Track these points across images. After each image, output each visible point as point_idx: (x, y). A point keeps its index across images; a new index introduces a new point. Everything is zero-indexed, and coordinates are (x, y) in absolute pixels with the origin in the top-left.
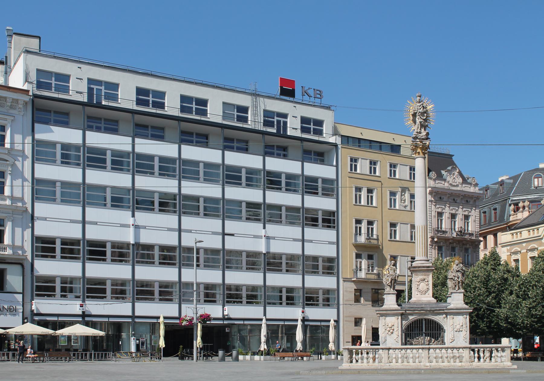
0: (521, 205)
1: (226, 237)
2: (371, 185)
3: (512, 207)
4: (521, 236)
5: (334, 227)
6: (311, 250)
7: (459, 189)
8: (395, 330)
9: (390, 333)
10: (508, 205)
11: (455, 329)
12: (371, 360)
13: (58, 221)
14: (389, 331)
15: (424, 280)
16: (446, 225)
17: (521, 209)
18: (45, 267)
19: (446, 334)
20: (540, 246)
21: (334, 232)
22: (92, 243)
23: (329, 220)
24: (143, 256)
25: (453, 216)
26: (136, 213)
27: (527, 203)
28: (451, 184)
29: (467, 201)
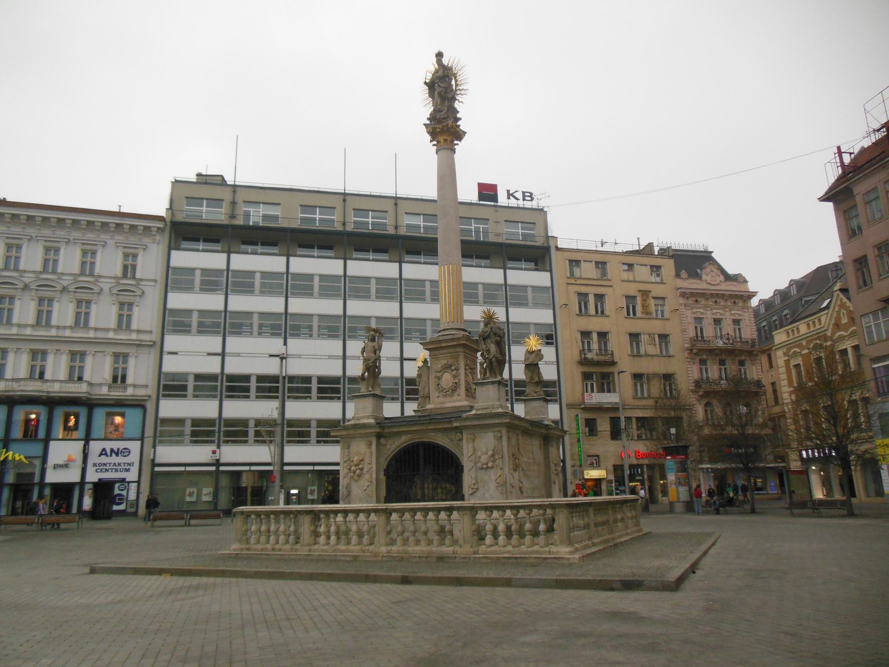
1: (405, 362)
2: (599, 290)
4: (798, 332)
8: (366, 470)
9: (355, 477)
11: (479, 465)
12: (282, 538)
13: (191, 354)
16: (709, 332)
18: (171, 408)
22: (232, 378)
24: (298, 390)
25: (717, 321)
26: (289, 341)
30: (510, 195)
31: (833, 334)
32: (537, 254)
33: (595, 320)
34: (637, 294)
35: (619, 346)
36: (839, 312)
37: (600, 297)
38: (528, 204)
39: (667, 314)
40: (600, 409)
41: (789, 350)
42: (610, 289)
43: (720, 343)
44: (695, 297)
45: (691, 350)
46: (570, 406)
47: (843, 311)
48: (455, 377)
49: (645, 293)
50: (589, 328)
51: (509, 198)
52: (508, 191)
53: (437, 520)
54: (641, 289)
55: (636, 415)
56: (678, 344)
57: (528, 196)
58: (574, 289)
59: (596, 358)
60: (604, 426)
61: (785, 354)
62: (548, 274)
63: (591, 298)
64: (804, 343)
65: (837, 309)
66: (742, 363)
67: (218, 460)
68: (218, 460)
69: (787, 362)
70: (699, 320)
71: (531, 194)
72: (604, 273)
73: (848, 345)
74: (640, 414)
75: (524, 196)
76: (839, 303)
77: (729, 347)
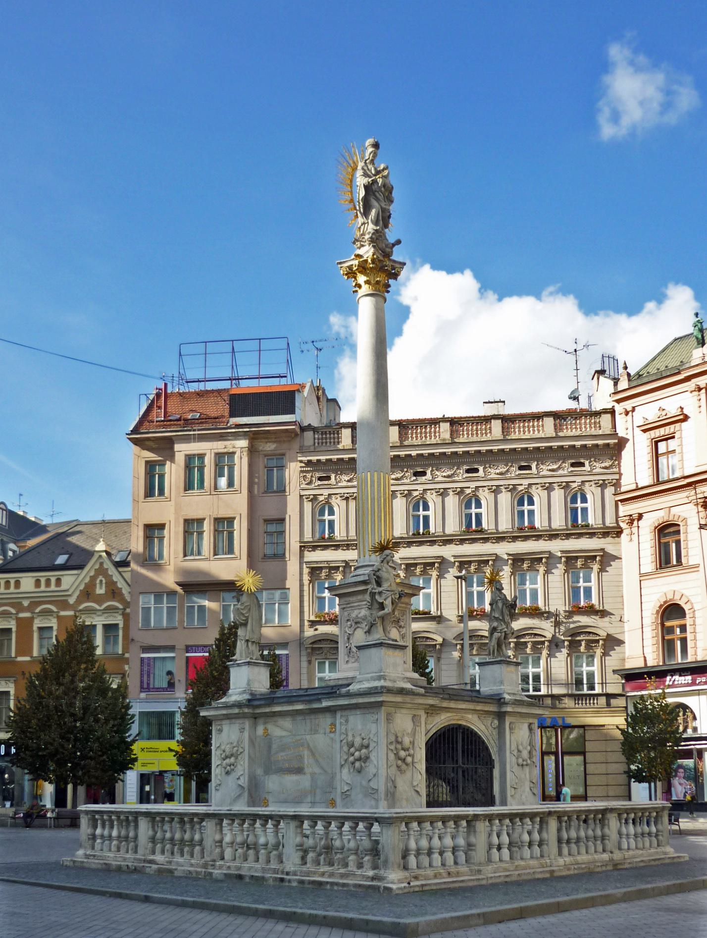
19: (496, 773)
20: (64, 609)
31: (79, 601)
36: (93, 579)
47: (101, 578)
53: (370, 835)
64: (26, 603)
65: (92, 573)
73: (99, 621)
76: (97, 566)
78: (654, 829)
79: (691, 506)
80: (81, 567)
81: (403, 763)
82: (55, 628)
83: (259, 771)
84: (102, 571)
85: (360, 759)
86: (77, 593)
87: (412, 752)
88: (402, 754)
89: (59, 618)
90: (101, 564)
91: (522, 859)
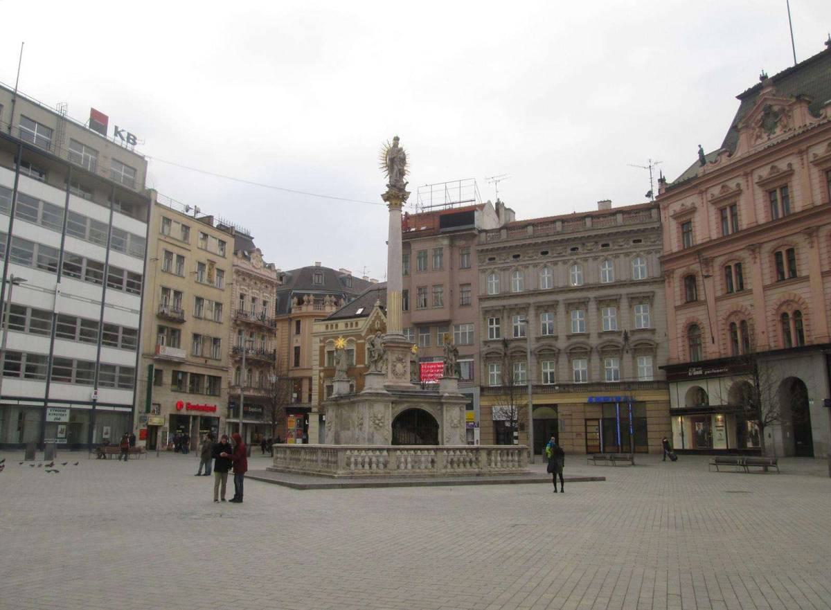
0: (305, 298)
2: (182, 253)
3: (295, 300)
5: (138, 293)
6: (111, 317)
7: (258, 271)
10: (289, 297)
14: (378, 425)
15: (402, 359)
16: (248, 307)
17: (305, 303)
19: (440, 430)
20: (359, 339)
21: (138, 299)
23: (135, 284)
25: (254, 300)
27: (312, 297)
28: (254, 266)
29: (266, 286)
30: (117, 132)
31: (367, 335)
32: (136, 201)
33: (173, 279)
34: (206, 262)
35: (188, 305)
36: (374, 322)
37: (181, 258)
38: (130, 147)
39: (224, 286)
40: (168, 362)
41: (326, 339)
42: (189, 253)
43: (252, 319)
44: (243, 275)
45: (236, 321)
46: (145, 356)
48: (404, 367)
49: (212, 263)
50: (169, 286)
51: (116, 135)
52: (116, 128)
54: (209, 258)
55: (192, 371)
56: (227, 313)
57: (132, 139)
58: (163, 245)
59: (170, 314)
60: (167, 378)
61: (321, 341)
62: (145, 225)
63: (175, 257)
65: (373, 319)
66: (263, 338)
67: (95, 400)
68: (95, 400)
69: (322, 349)
70: (242, 297)
71: (135, 138)
72: (186, 237)
74: (194, 370)
75: (128, 138)
76: (375, 315)
77: (260, 323)
78: (516, 459)
79: (698, 265)
80: (367, 315)
81: (378, 426)
82: (355, 349)
83: (339, 429)
84: (378, 317)
85: (360, 424)
86: (365, 331)
87: (382, 421)
88: (377, 422)
89: (357, 344)
90: (378, 313)
91: (419, 468)
